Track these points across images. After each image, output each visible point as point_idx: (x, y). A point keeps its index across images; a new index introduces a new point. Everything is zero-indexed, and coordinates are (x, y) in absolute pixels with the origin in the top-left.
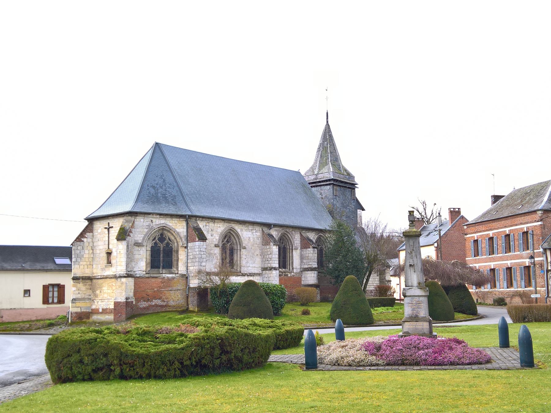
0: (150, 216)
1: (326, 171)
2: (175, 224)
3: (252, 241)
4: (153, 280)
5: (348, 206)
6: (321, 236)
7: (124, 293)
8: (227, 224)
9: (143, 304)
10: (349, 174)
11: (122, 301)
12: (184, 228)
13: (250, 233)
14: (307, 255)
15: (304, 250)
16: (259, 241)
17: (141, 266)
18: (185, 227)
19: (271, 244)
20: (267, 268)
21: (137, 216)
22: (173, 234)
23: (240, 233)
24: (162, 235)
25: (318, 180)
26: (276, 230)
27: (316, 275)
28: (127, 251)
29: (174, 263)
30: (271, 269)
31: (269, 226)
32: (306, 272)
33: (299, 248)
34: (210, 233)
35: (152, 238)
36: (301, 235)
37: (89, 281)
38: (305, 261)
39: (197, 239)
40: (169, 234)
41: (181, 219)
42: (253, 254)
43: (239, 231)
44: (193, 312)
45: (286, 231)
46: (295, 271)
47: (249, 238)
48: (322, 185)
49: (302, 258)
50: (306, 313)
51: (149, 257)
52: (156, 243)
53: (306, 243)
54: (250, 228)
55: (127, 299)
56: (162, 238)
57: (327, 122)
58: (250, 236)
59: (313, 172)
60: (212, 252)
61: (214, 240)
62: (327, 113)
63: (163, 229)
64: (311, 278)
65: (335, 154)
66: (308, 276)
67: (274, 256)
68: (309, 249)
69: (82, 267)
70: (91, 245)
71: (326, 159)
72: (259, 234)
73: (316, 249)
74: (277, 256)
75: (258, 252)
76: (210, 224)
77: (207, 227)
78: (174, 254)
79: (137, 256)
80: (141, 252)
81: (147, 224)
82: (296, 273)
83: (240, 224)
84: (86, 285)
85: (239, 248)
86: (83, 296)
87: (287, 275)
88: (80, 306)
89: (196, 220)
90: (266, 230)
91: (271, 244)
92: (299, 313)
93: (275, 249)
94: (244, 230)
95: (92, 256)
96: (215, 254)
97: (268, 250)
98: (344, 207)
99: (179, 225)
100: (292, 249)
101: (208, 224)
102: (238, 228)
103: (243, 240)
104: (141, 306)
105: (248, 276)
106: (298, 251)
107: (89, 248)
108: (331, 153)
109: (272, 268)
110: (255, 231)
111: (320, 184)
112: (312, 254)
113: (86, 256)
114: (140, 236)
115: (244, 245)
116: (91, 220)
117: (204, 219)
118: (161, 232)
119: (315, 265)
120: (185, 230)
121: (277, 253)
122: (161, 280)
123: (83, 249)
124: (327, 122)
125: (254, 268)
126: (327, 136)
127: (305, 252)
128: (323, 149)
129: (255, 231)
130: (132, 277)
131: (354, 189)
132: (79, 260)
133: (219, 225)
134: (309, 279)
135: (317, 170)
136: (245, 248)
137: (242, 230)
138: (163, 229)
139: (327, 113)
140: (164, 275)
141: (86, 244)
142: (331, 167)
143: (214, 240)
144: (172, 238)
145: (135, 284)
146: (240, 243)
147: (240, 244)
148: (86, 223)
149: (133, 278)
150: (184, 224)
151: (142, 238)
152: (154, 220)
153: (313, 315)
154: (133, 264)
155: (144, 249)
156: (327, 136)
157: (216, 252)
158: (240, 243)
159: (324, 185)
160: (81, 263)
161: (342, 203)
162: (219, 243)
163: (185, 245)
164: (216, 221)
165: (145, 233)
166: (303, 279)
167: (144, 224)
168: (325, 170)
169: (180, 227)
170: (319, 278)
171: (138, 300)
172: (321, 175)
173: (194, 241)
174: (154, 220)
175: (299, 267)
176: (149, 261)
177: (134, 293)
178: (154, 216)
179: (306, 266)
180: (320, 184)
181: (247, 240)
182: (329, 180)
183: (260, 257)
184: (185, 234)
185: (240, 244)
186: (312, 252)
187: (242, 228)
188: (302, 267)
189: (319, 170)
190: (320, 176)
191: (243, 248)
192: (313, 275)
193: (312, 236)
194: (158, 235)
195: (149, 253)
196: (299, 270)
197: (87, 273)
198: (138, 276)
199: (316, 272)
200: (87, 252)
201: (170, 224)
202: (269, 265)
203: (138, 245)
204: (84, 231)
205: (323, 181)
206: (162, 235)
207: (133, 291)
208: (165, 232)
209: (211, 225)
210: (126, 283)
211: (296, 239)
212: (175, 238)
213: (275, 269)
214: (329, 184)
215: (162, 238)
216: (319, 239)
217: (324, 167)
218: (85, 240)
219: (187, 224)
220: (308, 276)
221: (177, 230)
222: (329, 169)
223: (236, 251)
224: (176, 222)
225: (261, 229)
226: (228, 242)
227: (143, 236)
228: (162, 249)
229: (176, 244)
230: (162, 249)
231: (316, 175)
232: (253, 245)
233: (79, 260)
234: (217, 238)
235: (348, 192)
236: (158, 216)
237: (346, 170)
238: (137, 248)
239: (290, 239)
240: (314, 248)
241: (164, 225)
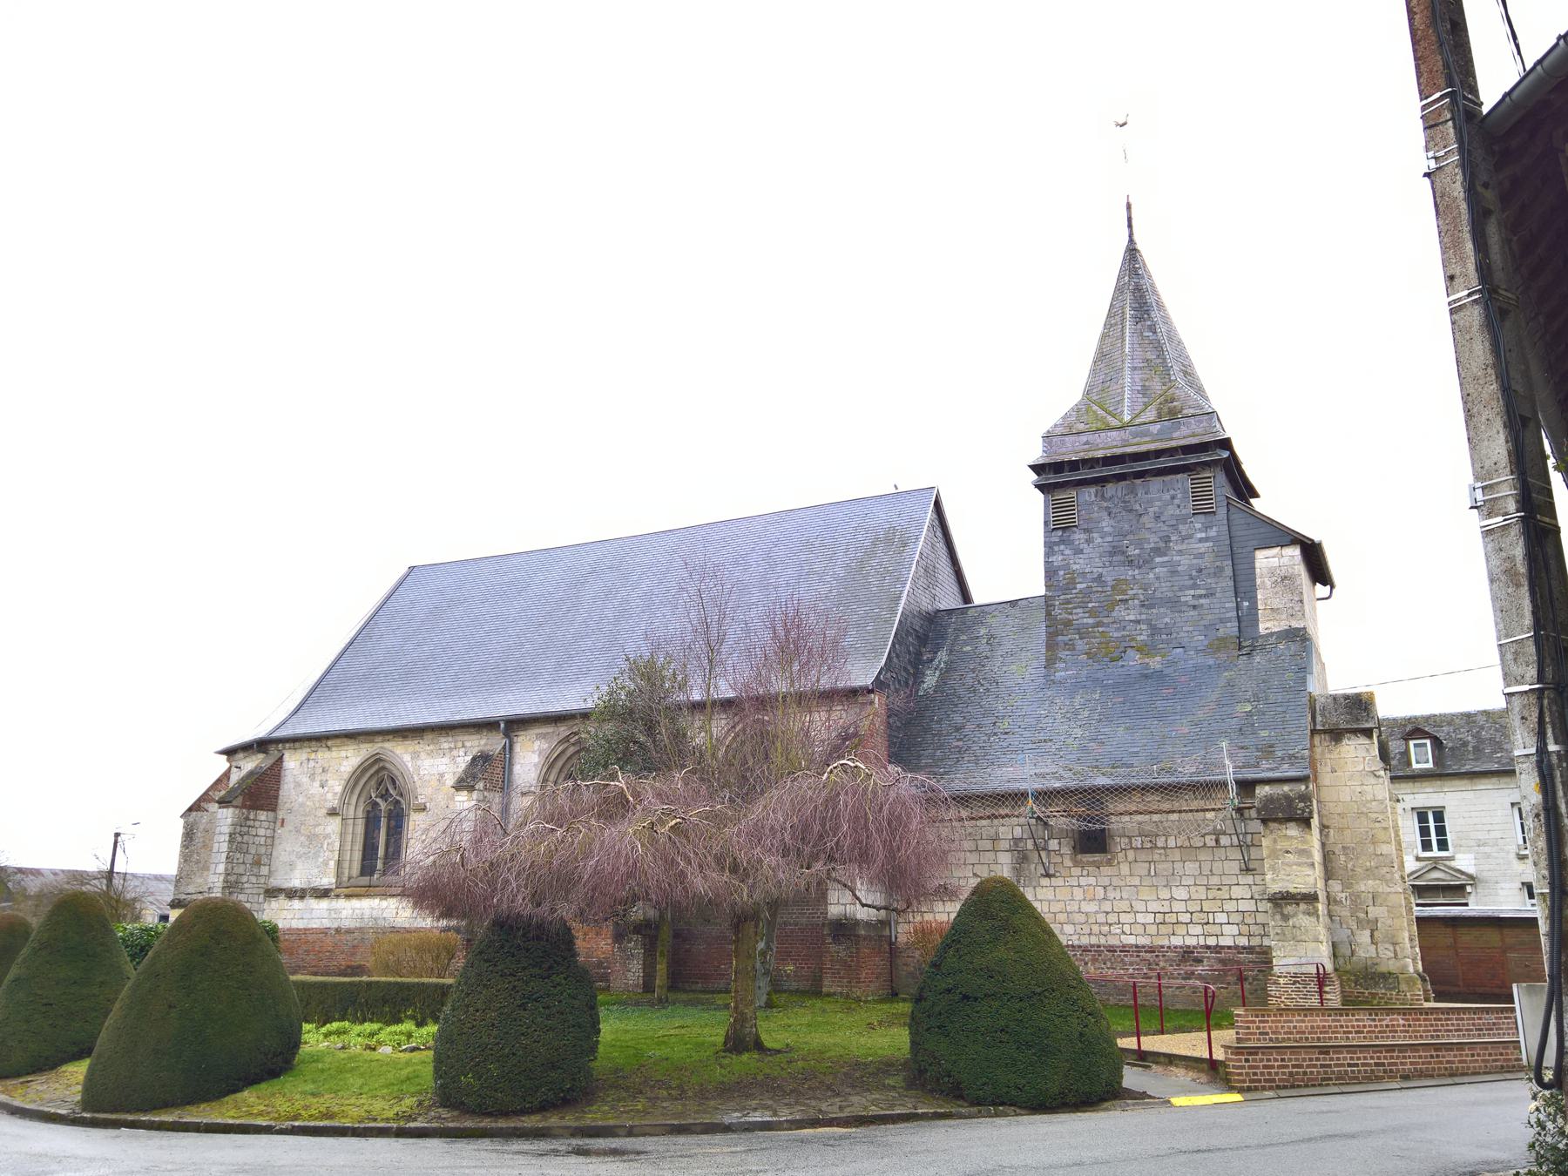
13: (446, 760)
26: (538, 736)
34: (318, 778)
47: (442, 775)
54: (446, 746)
57: (1131, 235)
58: (442, 768)
60: (319, 830)
61: (329, 796)
62: (1129, 207)
76: (320, 755)
77: (312, 764)
83: (405, 737)
94: (423, 755)
96: (327, 836)
102: (403, 755)
115: (421, 800)
124: (1131, 235)
126: (1136, 296)
133: (343, 754)
137: (416, 755)
139: (1129, 207)
143: (329, 796)
156: (1136, 296)
157: (329, 829)
164: (330, 743)
181: (434, 783)
187: (417, 748)
191: (416, 810)
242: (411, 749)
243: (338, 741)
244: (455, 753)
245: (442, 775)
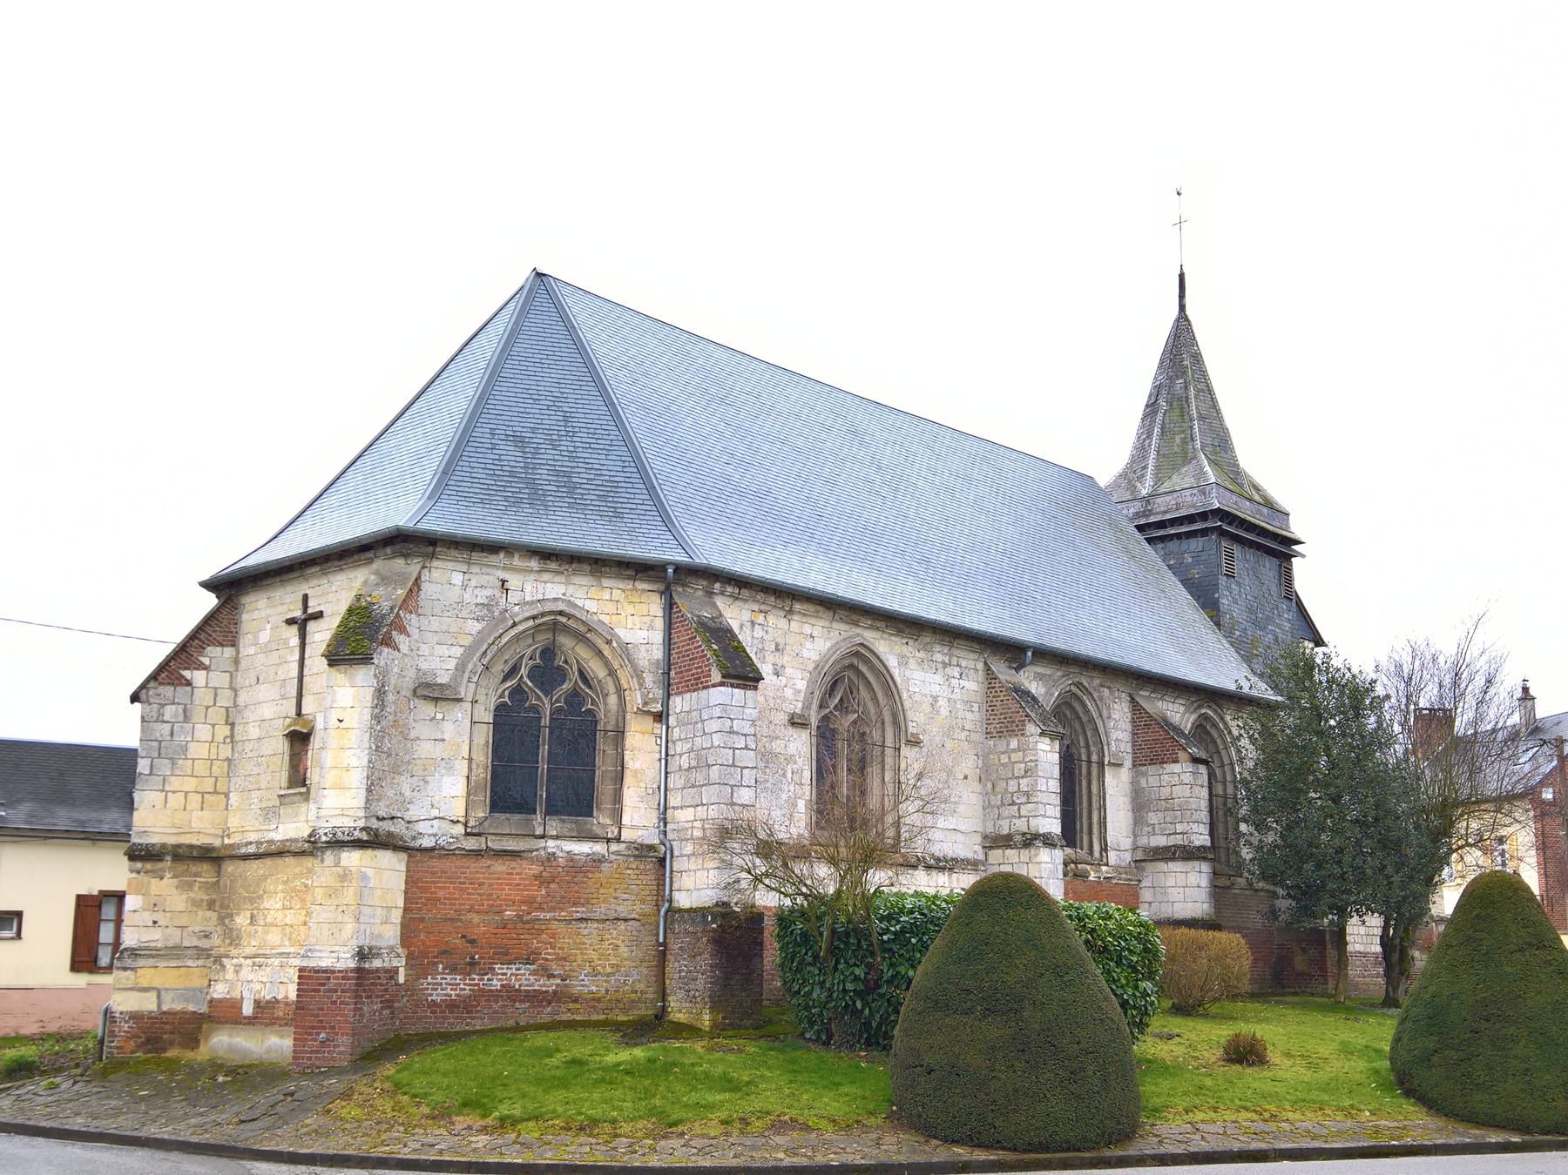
0: (493, 559)
1: (1189, 481)
2: (610, 608)
3: (944, 712)
4: (500, 867)
5: (1269, 619)
6: (1206, 717)
7: (349, 928)
8: (843, 626)
9: (445, 986)
10: (1269, 504)
11: (340, 966)
12: (651, 628)
13: (938, 678)
14: (1165, 792)
15: (1151, 769)
16: (972, 717)
17: (444, 796)
18: (659, 623)
19: (1031, 728)
20: (1009, 837)
21: (433, 556)
22: (600, 653)
23: (896, 673)
24: (548, 653)
25: (1152, 519)
27: (1204, 881)
28: (377, 718)
29: (604, 788)
30: (1031, 840)
31: (1013, 651)
32: (1162, 866)
33: (1128, 763)
35: (500, 668)
36: (1135, 706)
37: (205, 867)
38: (1153, 818)
39: (716, 676)
40: (583, 652)
41: (640, 585)
42: (950, 773)
43: (892, 662)
44: (687, 1031)
45: (1079, 685)
46: (1113, 857)
47: (935, 698)
48: (1171, 537)
49: (1140, 804)
50: (1245, 1054)
51: (483, 758)
52: (517, 692)
53: (1155, 745)
54: (939, 657)
55: (362, 954)
56: (548, 671)
57: (1182, 307)
58: (936, 689)
59: (1132, 488)
60: (777, 746)
61: (789, 692)
62: (1182, 277)
63: (556, 625)
64: (1184, 891)
65: (1215, 423)
66: (1171, 882)
67: (1042, 785)
68: (1176, 768)
69: (176, 801)
70: (225, 699)
71: (1184, 442)
72: (972, 685)
73: (1203, 769)
74: (1054, 785)
75: (969, 765)
76: (771, 619)
78: (603, 746)
79: (425, 749)
80: (448, 730)
81: (482, 596)
82: (1117, 868)
83: (900, 632)
84: (190, 886)
85: (889, 741)
86: (175, 937)
87: (1085, 876)
88: (157, 982)
89: (710, 594)
90: (1001, 669)
91: (1031, 728)
92: (1213, 1055)
93: (1047, 754)
94: (912, 663)
95: (226, 751)
96: (790, 759)
97: (1015, 757)
98: (1256, 623)
99: (630, 609)
100: (1101, 765)
101: (760, 619)
103: (907, 704)
104: (437, 996)
105: (928, 867)
106: (1125, 774)
107: (217, 715)
108: (1202, 418)
109: (1036, 836)
110: (956, 672)
111: (1162, 533)
112: (1183, 783)
113: (198, 750)
114: (443, 650)
116: (232, 587)
117: (745, 593)
118: (544, 638)
119: (1201, 838)
120: (658, 637)
121: (1056, 772)
122: (535, 869)
123: (186, 718)
124: (1182, 307)
125: (952, 836)
127: (1153, 781)
128: (1170, 403)
129: (956, 672)
130: (396, 848)
131: (1288, 557)
132: (164, 767)
133: (807, 629)
134: (1175, 894)
135: (1149, 481)
136: (915, 742)
138: (555, 627)
139: (1182, 277)
140: (551, 843)
141: (202, 697)
142: (1207, 468)
143: (789, 692)
144: (597, 669)
145: (411, 881)
146: (895, 716)
147: (896, 723)
148: (210, 601)
149: (404, 856)
150: (655, 606)
151: (452, 664)
152: (514, 581)
153: (1284, 1069)
154: (406, 784)
155: (461, 713)
157: (793, 748)
158: (895, 716)
159: (1178, 536)
160: (175, 783)
161: (1251, 611)
162: (807, 707)
163: (658, 707)
164: (797, 606)
165: (467, 641)
166: (1146, 895)
167: (468, 597)
168: (1182, 479)
169: (633, 621)
170: (1219, 891)
171: (420, 963)
172: (1168, 498)
173: (699, 683)
174: (514, 581)
175: (1127, 843)
176: (483, 774)
177: (405, 925)
178: (517, 561)
179: (1160, 841)
180: (1162, 533)
181: (926, 707)
182: (1204, 516)
183: (978, 787)
184: (658, 654)
185: (896, 723)
186: (1187, 778)
188: (1143, 841)
189: (1158, 479)
190: (1161, 503)
192: (1194, 878)
193: (1178, 713)
194: (529, 652)
195: (484, 735)
196: (1128, 857)
197: (201, 828)
198: (427, 843)
199: (1205, 867)
200: (203, 732)
201: (591, 606)
202: (1021, 825)
203: (433, 693)
204: (193, 636)
205: (1174, 522)
206: (548, 653)
207: (397, 916)
208: (565, 641)
209: (776, 621)
210: (364, 877)
211: (1117, 723)
212: (612, 673)
213: (1048, 841)
214: (1204, 532)
215: (548, 671)
216: (1202, 731)
217: (1175, 468)
218: (198, 677)
219: (670, 606)
220: (1171, 882)
221: (620, 632)
222: (1201, 473)
223: (877, 751)
224: (617, 594)
225: (980, 666)
226: (842, 707)
227: (458, 651)
228: (545, 721)
229: (613, 700)
230: (545, 721)
231: (1147, 500)
232: (948, 732)
233: (164, 767)
234: (802, 685)
235: (1269, 567)
236: (534, 564)
237: (1256, 488)
238: (427, 709)
239: (1092, 720)
240: (1196, 760)
241: (561, 607)
242: (897, 649)
243: (811, 608)
244: (949, 670)
245: (935, 698)
